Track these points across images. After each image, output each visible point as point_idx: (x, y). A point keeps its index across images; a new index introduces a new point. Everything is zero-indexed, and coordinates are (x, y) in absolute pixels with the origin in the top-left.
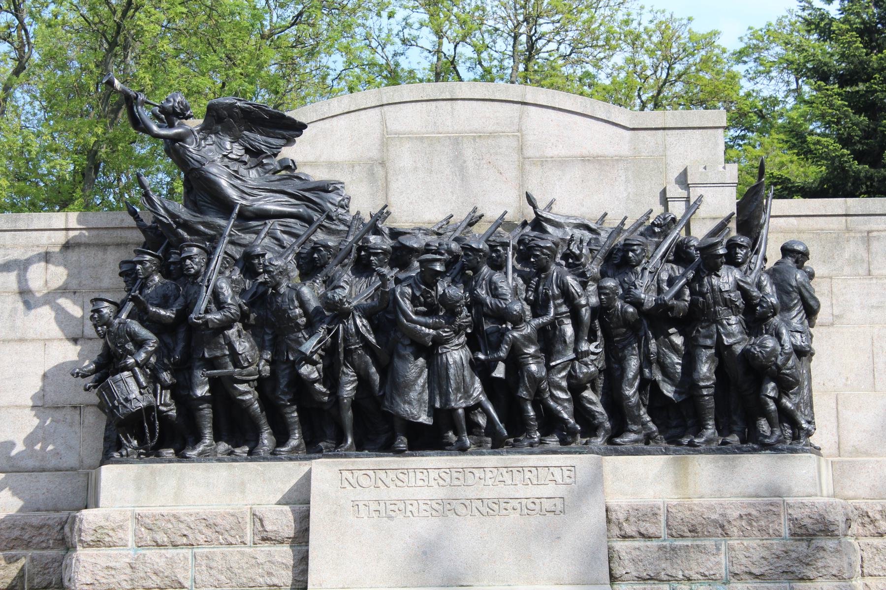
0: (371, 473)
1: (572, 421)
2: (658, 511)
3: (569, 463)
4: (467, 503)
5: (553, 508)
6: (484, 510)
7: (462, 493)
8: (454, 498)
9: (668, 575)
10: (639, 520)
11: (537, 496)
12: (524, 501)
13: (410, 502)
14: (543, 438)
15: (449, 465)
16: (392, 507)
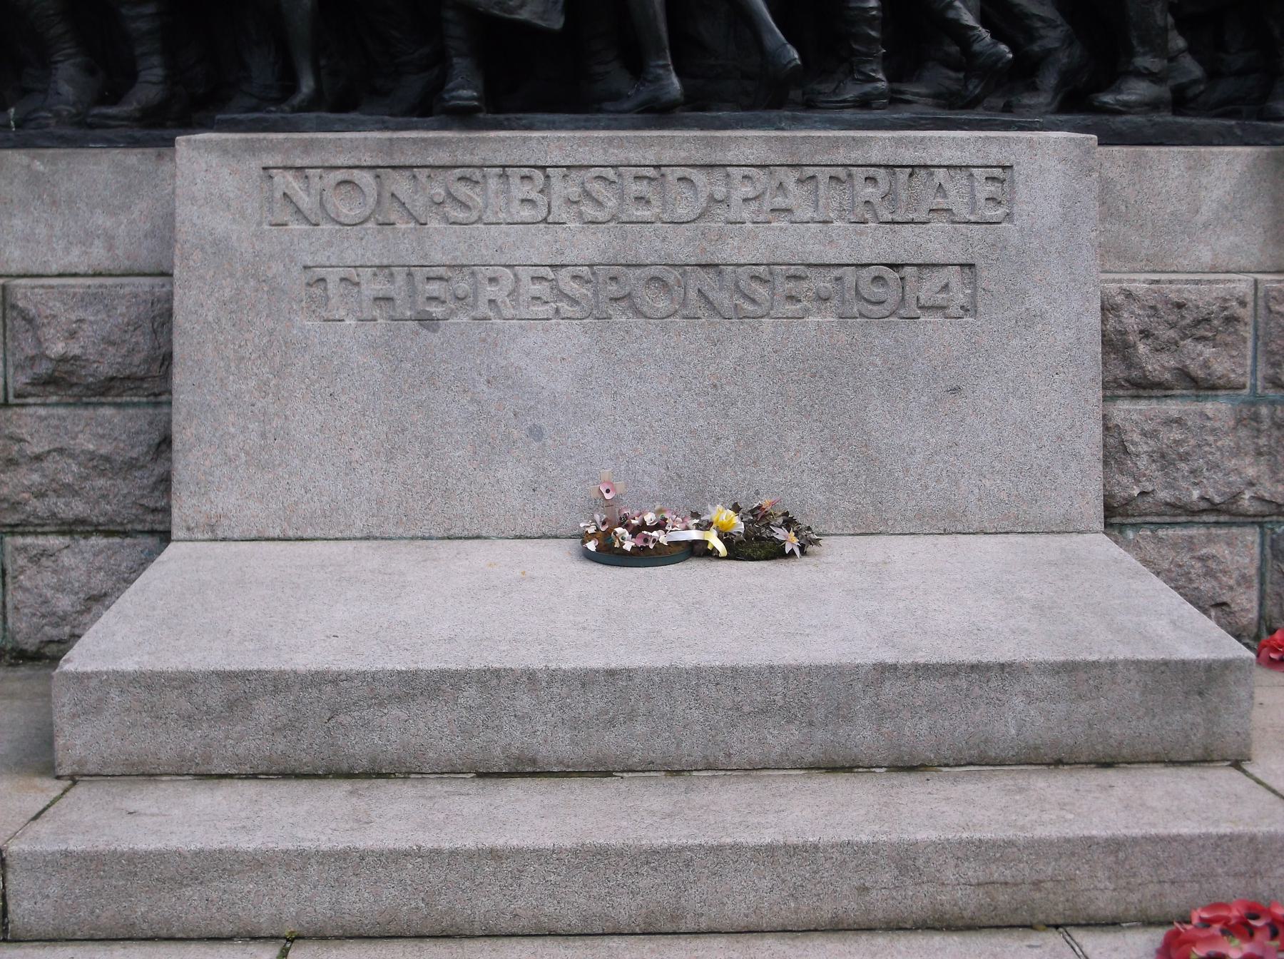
0: (365, 178)
1: (985, 34)
2: (1240, 312)
3: (995, 154)
4: (672, 276)
5: (940, 299)
6: (724, 299)
7: (658, 244)
8: (631, 259)
9: (1261, 499)
10: (1184, 337)
11: (892, 260)
12: (849, 275)
13: (490, 272)
14: (896, 86)
15: (617, 155)
16: (434, 288)
